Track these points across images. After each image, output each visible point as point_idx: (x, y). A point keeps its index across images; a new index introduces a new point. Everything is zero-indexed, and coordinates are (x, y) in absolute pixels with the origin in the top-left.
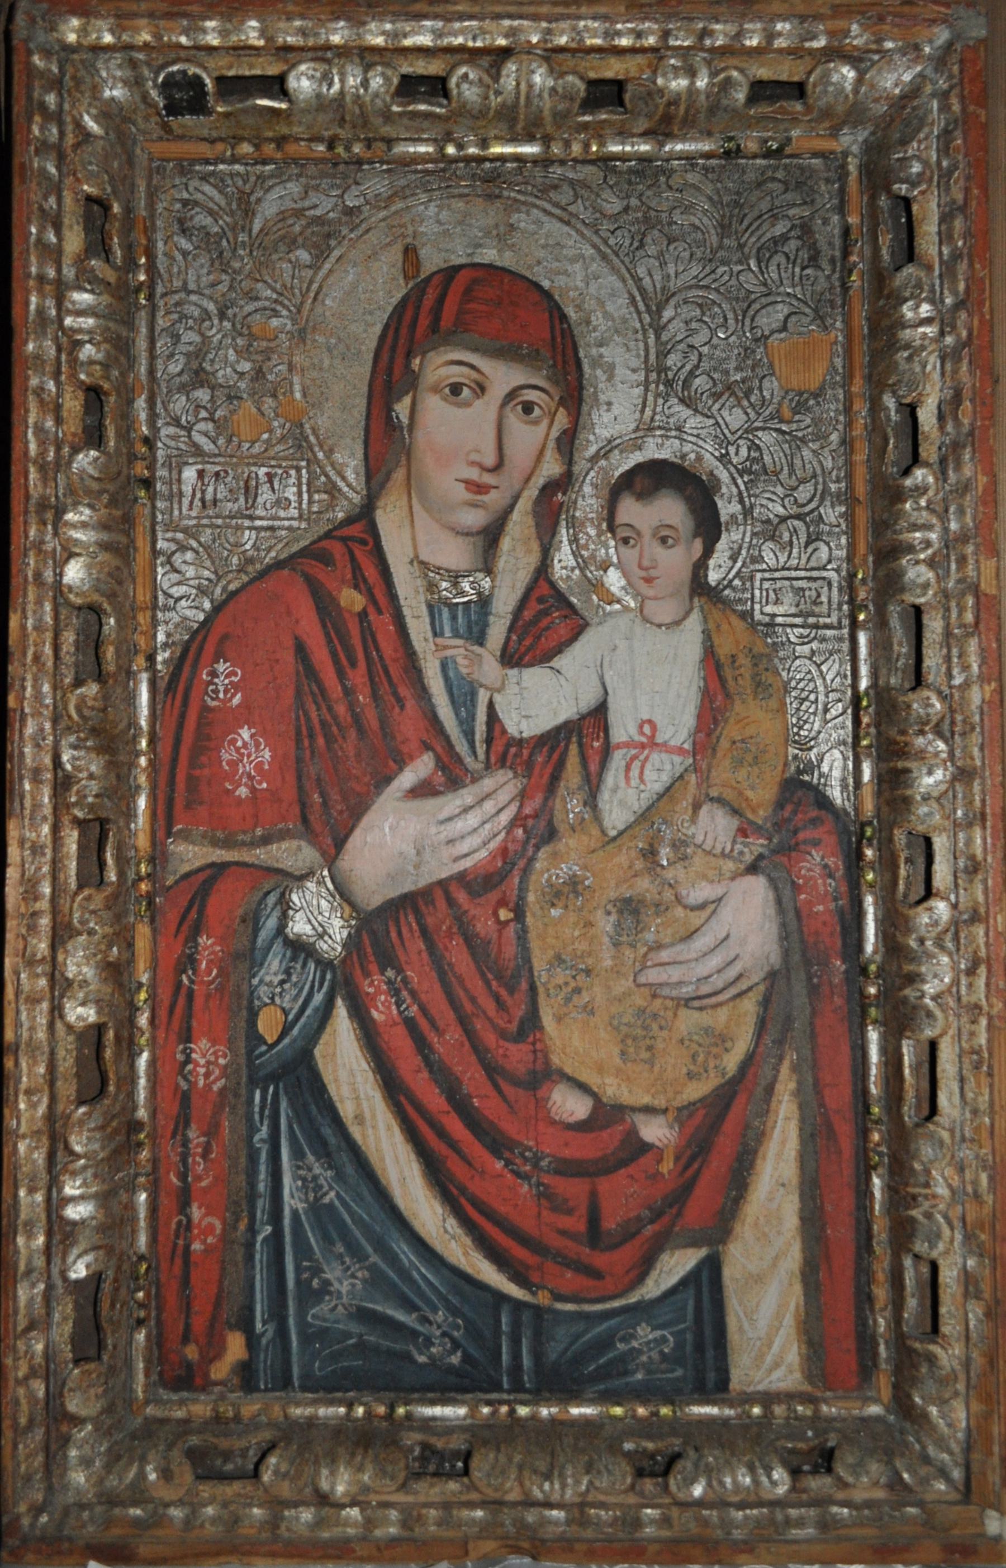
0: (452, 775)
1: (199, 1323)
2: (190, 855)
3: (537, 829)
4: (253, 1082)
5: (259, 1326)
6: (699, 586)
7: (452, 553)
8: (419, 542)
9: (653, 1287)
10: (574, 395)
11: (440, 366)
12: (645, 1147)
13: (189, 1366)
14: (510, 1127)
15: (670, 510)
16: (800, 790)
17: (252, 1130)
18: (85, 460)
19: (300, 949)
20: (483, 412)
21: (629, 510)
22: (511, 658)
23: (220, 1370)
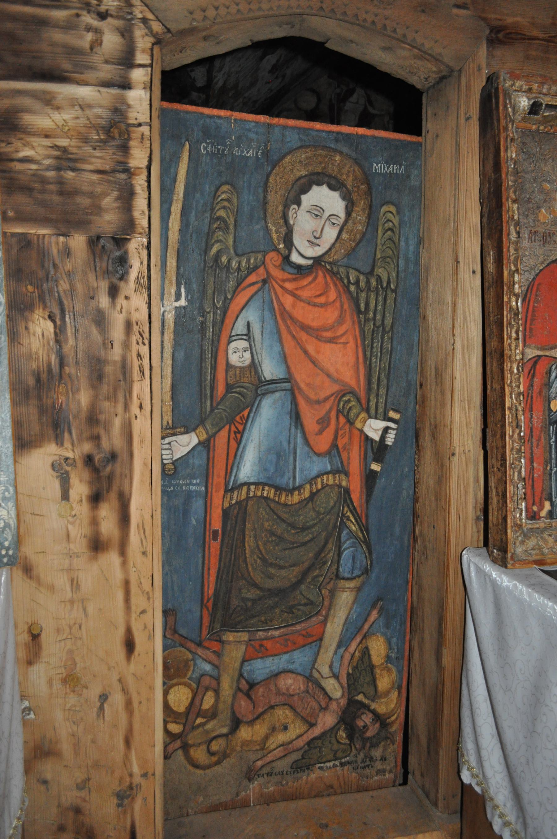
1: (537, 500)
4: (550, 424)
5: (554, 499)
13: (535, 512)
17: (550, 439)
23: (543, 513)
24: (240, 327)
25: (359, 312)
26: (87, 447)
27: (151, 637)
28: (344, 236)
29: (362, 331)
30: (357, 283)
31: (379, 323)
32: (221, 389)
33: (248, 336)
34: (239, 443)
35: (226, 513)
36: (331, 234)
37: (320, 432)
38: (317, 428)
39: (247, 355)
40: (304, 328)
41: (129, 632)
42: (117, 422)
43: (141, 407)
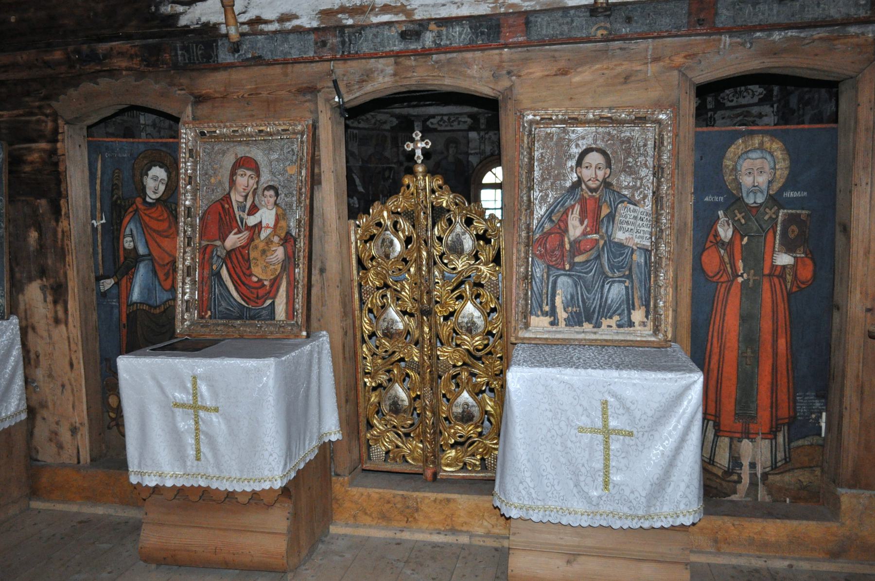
0: (239, 232)
2: (204, 243)
3: (251, 239)
4: (213, 275)
6: (276, 204)
7: (241, 199)
8: (236, 198)
9: (265, 305)
10: (258, 176)
11: (240, 172)
12: (264, 285)
14: (246, 282)
15: (272, 192)
16: (288, 233)
18: (188, 187)
19: (219, 257)
20: (246, 178)
21: (266, 193)
22: (249, 215)
24: (128, 231)
26: (52, 281)
27: (79, 363)
32: (122, 259)
33: (132, 235)
34: (131, 283)
35: (128, 315)
36: (162, 188)
37: (166, 280)
38: (164, 278)
39: (132, 244)
40: (154, 231)
41: (71, 359)
42: (62, 272)
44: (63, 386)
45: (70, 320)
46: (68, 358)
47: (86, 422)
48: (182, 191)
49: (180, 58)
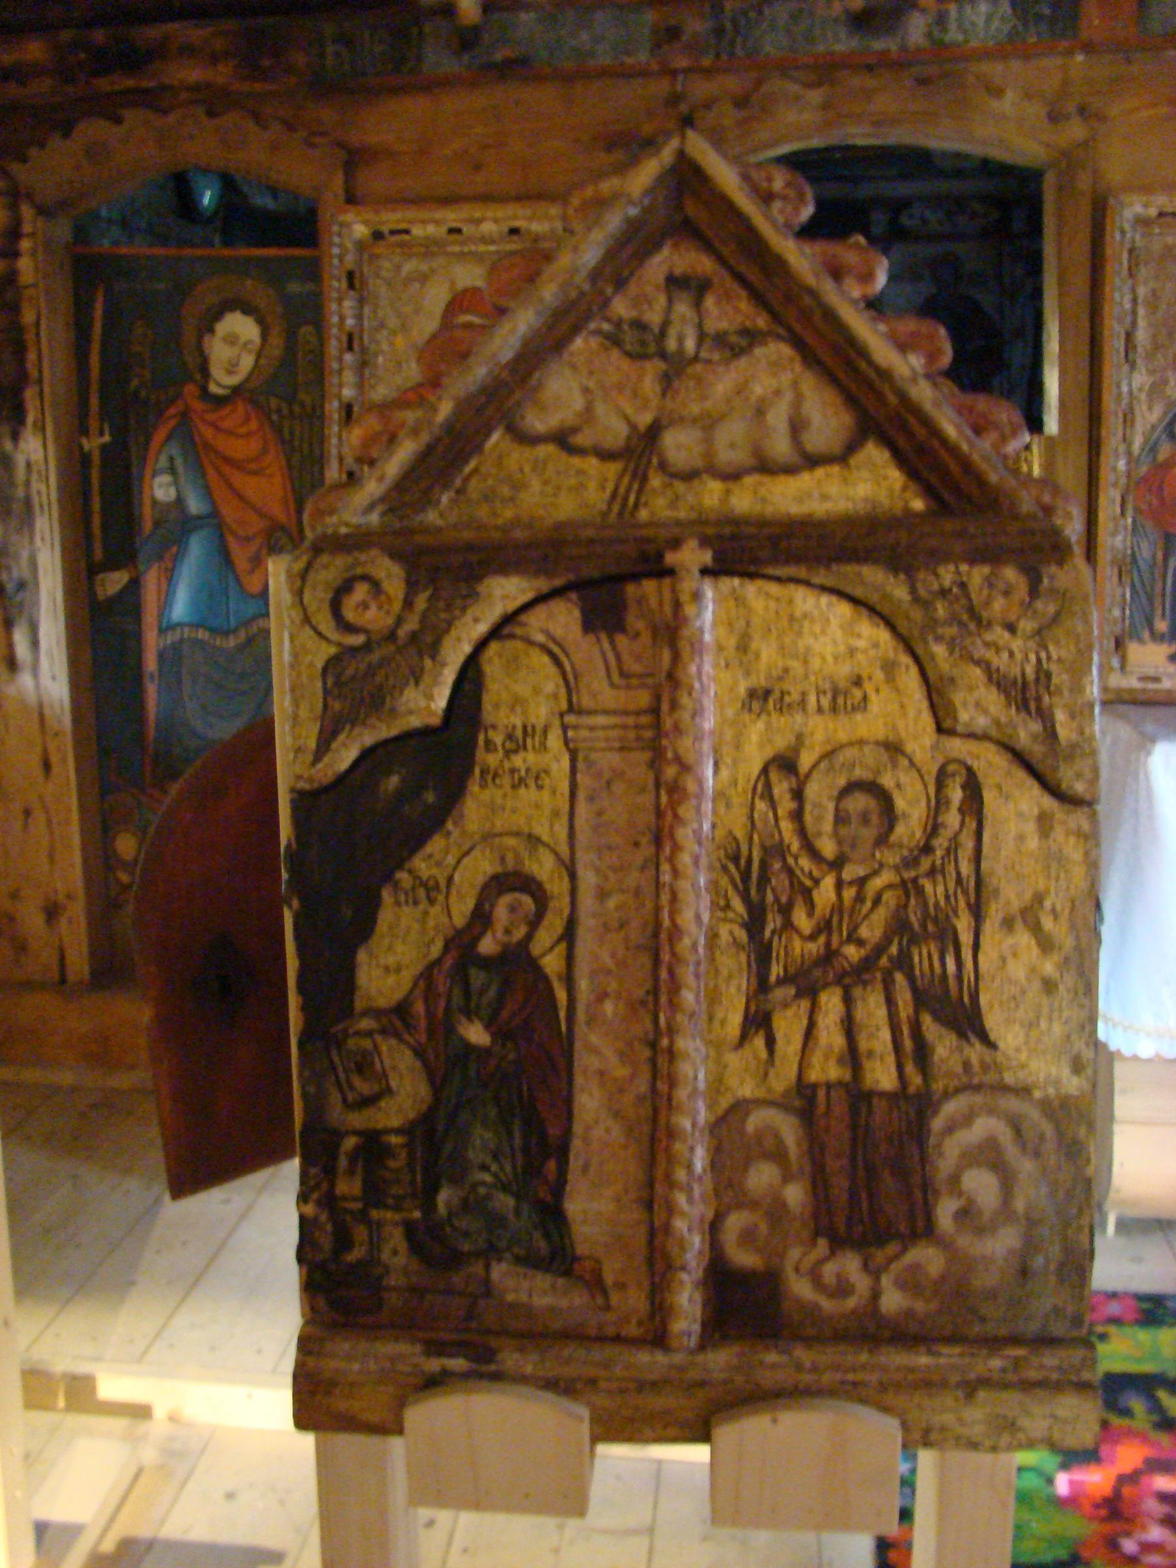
24: (163, 461)
25: (283, 442)
27: (64, 759)
28: (262, 362)
29: (289, 461)
30: (279, 411)
31: (306, 451)
36: (247, 362)
37: (252, 571)
40: (228, 460)
42: (25, 554)
43: (43, 539)
44: (27, 813)
45: (44, 664)
46: (39, 749)
47: (81, 893)
48: (335, 366)
49: (330, 61)
